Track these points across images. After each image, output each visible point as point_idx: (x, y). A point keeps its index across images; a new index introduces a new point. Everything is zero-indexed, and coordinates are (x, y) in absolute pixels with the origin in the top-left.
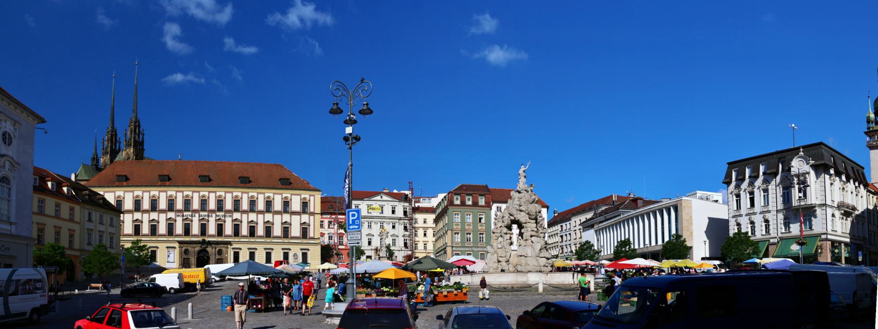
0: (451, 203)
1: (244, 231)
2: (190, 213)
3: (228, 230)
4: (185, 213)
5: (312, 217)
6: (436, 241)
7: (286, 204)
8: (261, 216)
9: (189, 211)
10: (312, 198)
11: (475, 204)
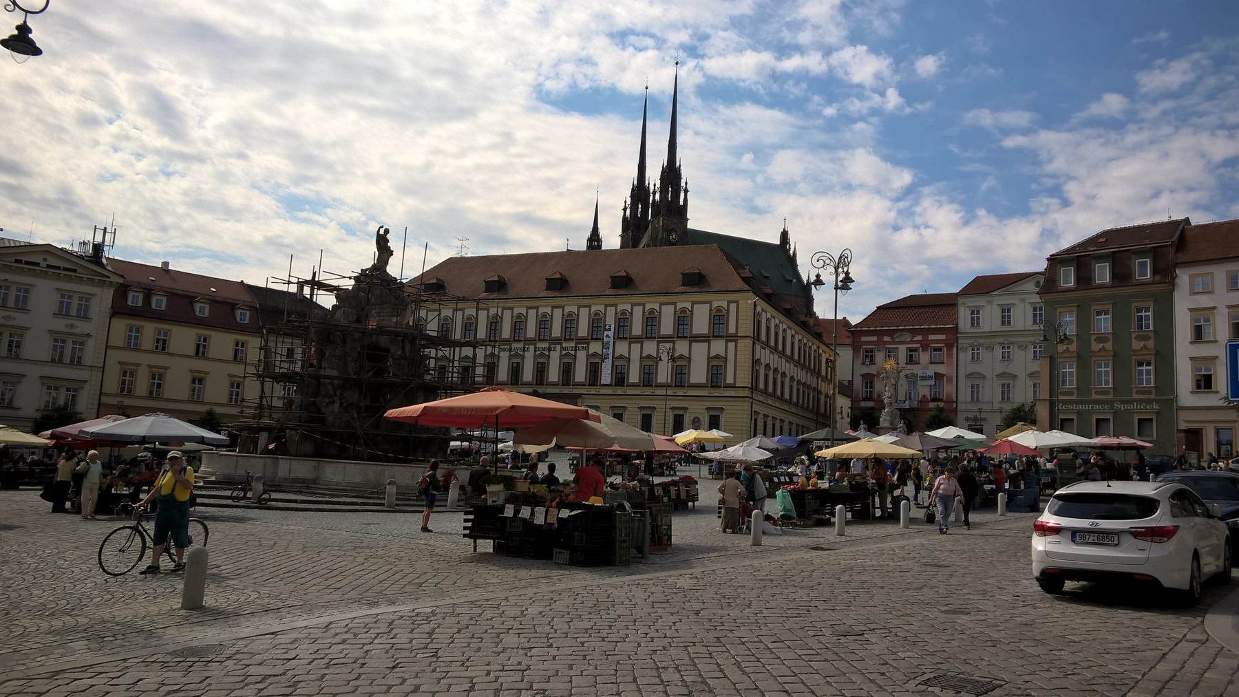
1: (606, 376)
2: (521, 345)
3: (580, 374)
4: (514, 346)
5: (731, 345)
7: (683, 319)
8: (636, 347)
9: (519, 341)
10: (733, 307)
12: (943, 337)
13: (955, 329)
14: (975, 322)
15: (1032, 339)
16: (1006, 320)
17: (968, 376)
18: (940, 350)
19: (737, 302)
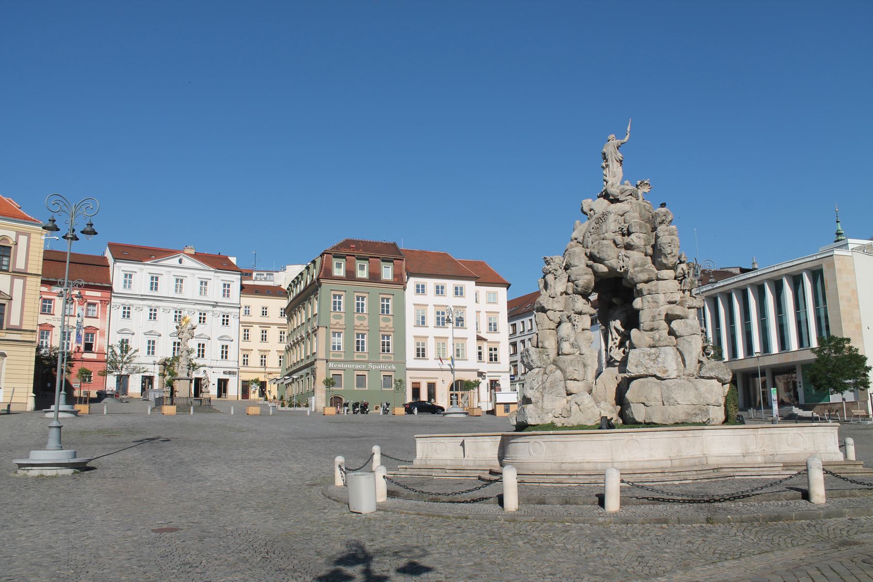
0: (327, 273)
5: (18, 282)
6: (289, 349)
10: (23, 240)
11: (374, 277)
12: (98, 294)
13: (110, 289)
14: (128, 283)
15: (175, 305)
16: (154, 286)
17: (120, 332)
18: (94, 304)
19: (28, 235)
